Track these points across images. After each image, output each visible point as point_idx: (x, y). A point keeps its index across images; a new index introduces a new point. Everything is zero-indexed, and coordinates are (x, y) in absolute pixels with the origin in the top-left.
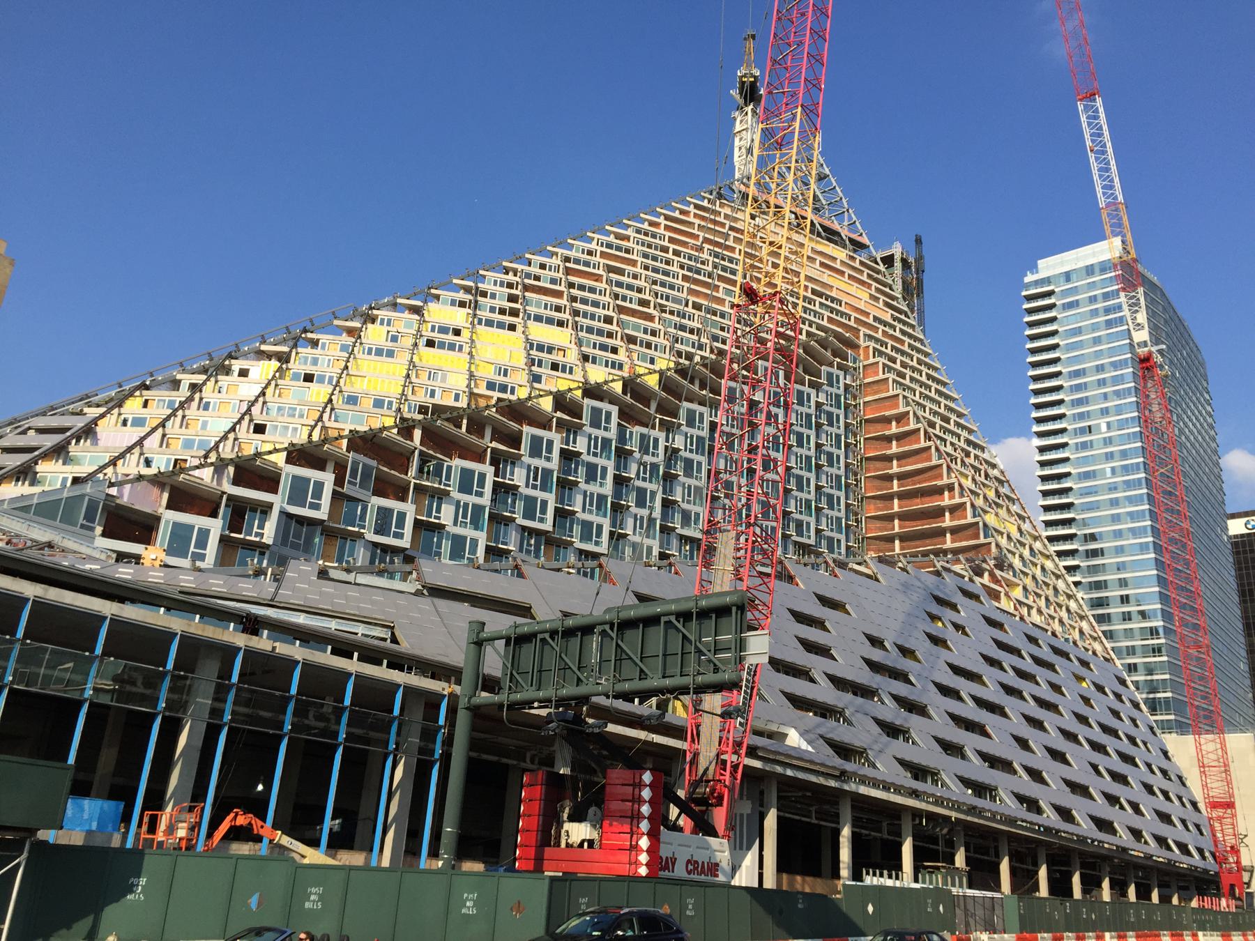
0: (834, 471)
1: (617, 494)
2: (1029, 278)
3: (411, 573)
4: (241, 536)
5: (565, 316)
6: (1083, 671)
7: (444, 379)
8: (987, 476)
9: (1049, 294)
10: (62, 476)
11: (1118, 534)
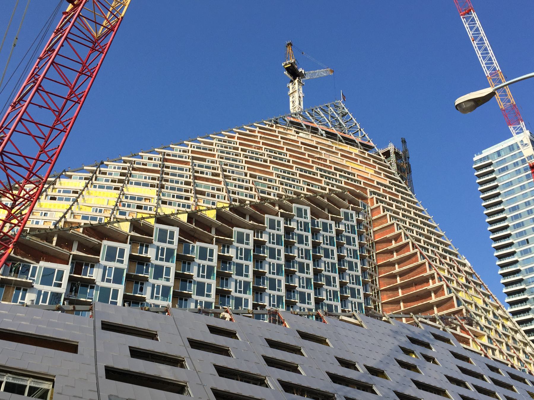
8: (459, 270)
9: (490, 164)
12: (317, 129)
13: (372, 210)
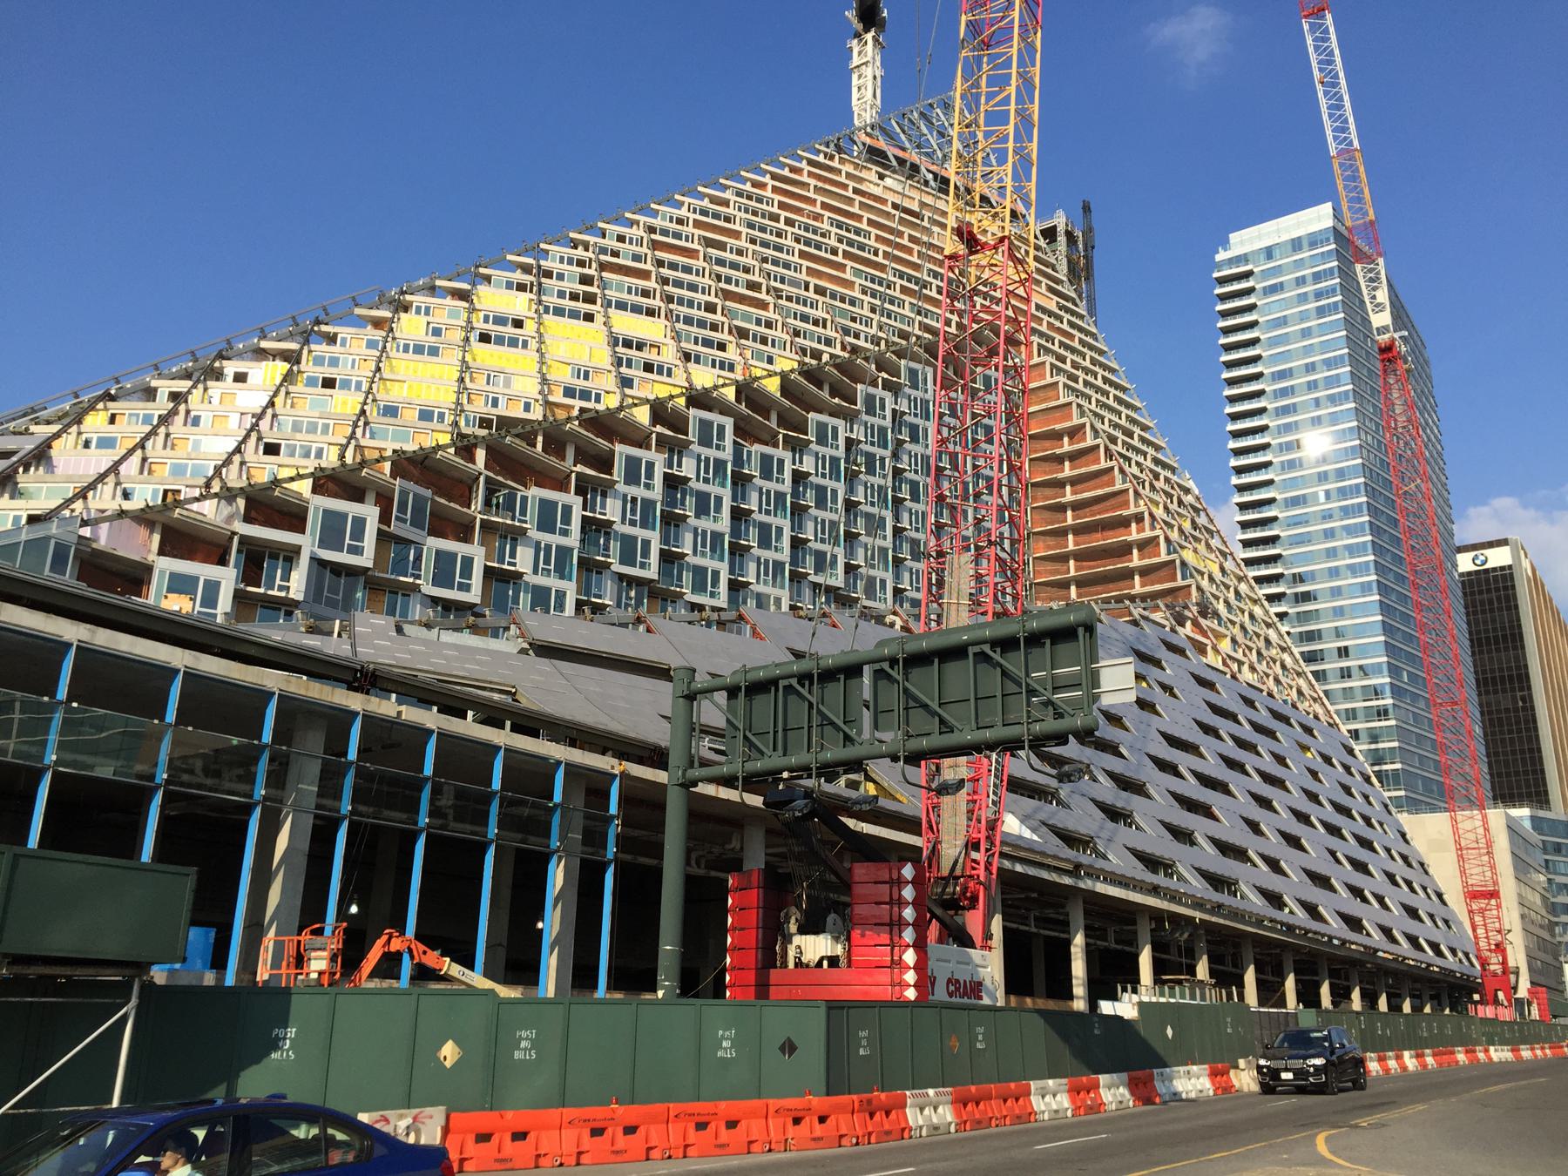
1: (735, 532)
2: (1221, 256)
3: (507, 629)
4: (262, 590)
5: (656, 303)
6: (1306, 739)
7: (507, 384)
8: (1180, 503)
9: (1247, 275)
10: (13, 514)
11: (1334, 573)
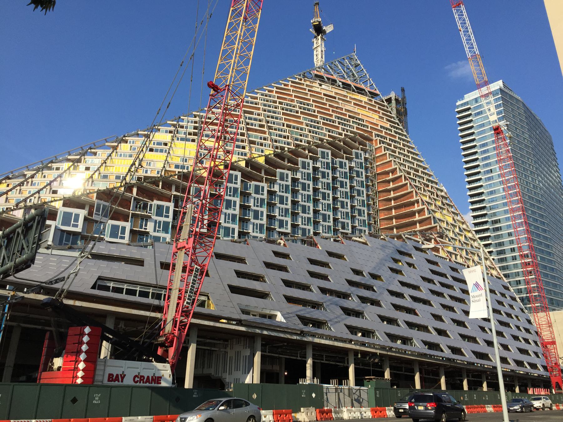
0: (360, 198)
7: (154, 166)
8: (437, 196)
9: (469, 109)
12: (335, 81)
13: (376, 149)
